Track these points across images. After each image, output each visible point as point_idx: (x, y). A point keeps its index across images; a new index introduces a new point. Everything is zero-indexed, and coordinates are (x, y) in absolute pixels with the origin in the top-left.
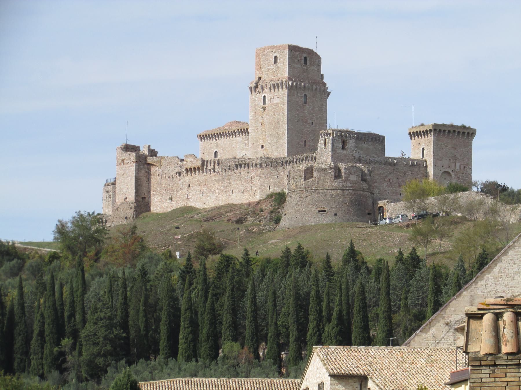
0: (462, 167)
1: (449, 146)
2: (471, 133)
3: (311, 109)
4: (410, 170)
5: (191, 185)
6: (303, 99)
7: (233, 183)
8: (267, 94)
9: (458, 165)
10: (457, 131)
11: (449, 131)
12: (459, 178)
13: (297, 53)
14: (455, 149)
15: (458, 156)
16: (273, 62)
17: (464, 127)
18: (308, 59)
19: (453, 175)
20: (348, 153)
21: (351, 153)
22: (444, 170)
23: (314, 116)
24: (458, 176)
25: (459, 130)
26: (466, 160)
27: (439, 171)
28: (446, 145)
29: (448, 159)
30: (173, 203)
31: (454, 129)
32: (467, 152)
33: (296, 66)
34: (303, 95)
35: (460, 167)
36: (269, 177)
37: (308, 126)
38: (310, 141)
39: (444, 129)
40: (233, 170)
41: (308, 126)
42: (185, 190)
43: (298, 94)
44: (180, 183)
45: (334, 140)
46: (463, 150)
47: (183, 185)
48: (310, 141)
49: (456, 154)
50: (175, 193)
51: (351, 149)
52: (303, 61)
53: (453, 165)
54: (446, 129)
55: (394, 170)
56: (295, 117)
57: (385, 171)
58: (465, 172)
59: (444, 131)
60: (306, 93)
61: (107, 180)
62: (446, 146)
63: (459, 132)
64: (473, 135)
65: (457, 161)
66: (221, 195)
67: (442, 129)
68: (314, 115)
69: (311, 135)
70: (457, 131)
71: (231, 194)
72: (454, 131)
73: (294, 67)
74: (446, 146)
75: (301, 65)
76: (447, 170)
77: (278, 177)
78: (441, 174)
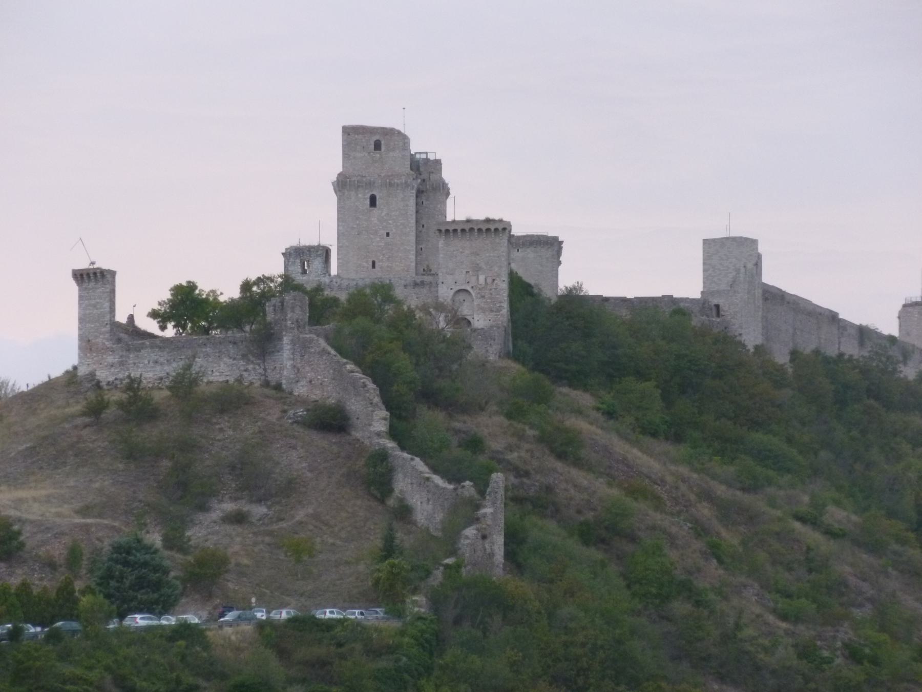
0: (489, 280)
1: (467, 252)
2: (500, 229)
3: (383, 214)
4: (415, 294)
6: (368, 202)
9: (482, 278)
10: (476, 228)
11: (463, 230)
12: (483, 297)
13: (360, 137)
14: (478, 255)
15: (483, 265)
17: (488, 221)
18: (383, 142)
19: (473, 294)
20: (311, 278)
21: (317, 279)
23: (390, 224)
24: (483, 294)
25: (479, 227)
26: (496, 269)
28: (461, 250)
31: (471, 226)
32: (498, 257)
33: (359, 155)
34: (368, 196)
35: (486, 280)
37: (378, 239)
38: (382, 260)
39: (453, 229)
41: (378, 239)
43: (357, 195)
45: (289, 262)
46: (492, 255)
48: (382, 260)
49: (478, 262)
51: (317, 272)
52: (372, 147)
53: (473, 279)
54: (456, 228)
56: (353, 228)
58: (494, 287)
59: (455, 231)
60: (374, 193)
61: (906, 299)
62: (462, 252)
63: (480, 230)
67: (451, 228)
68: (390, 222)
69: (384, 252)
70: (476, 228)
72: (472, 229)
73: (355, 158)
74: (462, 252)
75: (369, 153)
76: (463, 287)
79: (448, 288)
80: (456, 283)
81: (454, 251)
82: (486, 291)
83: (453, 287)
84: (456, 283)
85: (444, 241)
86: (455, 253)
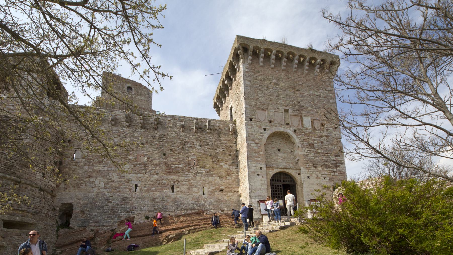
9: (307, 121)
12: (311, 145)
22: (274, 129)
27: (263, 131)
28: (274, 81)
29: (282, 109)
46: (316, 93)
49: (300, 99)
53: (295, 121)
55: (153, 137)
57: (128, 140)
64: (335, 67)
65: (304, 113)
76: (281, 129)
78: (266, 136)
79: (260, 127)
80: (270, 122)
81: (264, 80)
82: (313, 138)
83: (267, 127)
84: (270, 122)
85: (249, 64)
86: (265, 82)
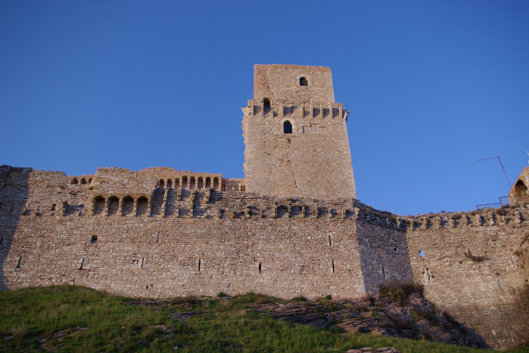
5: (100, 238)
7: (260, 246)
8: (295, 120)
16: (299, 83)
30: (23, 275)
36: (379, 247)
40: (264, 217)
42: (78, 248)
44: (59, 228)
47: (71, 235)
50: (35, 252)
66: (213, 272)
71: (252, 273)
77: (395, 249)
